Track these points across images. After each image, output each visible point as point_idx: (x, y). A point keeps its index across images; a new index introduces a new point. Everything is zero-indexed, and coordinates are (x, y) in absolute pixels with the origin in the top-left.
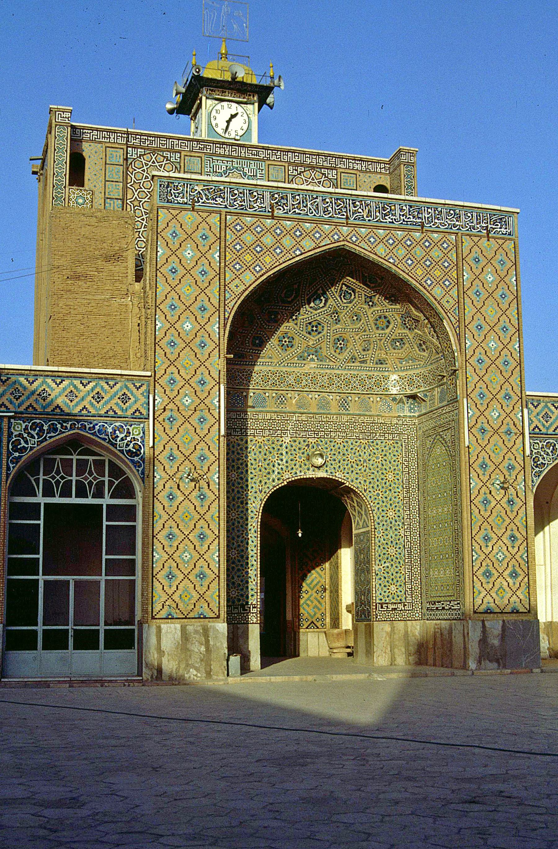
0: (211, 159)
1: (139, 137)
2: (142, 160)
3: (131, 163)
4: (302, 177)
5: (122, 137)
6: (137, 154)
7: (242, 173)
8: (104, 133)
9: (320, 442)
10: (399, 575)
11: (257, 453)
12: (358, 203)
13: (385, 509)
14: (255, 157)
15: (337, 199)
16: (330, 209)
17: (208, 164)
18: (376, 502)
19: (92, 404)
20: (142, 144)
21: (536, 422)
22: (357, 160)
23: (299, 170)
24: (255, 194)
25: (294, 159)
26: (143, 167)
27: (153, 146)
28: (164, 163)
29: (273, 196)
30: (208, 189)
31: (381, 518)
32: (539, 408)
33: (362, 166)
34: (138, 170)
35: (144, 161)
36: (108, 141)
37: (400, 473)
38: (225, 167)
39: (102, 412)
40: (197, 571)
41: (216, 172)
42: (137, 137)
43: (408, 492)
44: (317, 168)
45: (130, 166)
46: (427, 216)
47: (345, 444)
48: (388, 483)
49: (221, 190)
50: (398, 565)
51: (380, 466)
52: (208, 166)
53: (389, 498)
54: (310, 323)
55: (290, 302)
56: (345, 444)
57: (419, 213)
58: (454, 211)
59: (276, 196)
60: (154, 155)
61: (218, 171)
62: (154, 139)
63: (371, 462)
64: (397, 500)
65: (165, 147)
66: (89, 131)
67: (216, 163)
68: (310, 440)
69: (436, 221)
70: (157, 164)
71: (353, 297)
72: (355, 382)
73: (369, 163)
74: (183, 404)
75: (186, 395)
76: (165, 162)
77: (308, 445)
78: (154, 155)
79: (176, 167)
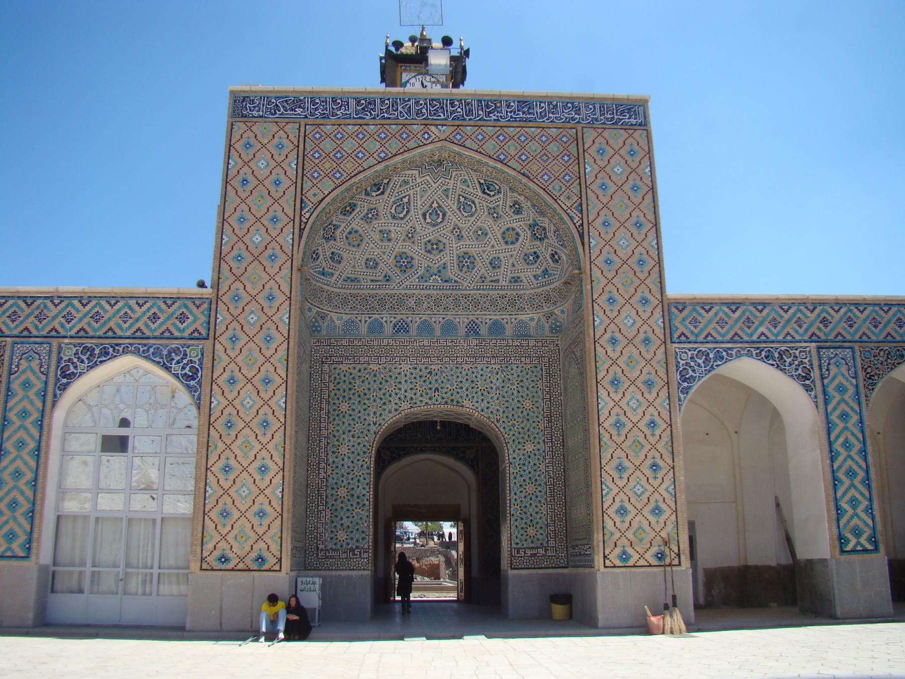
9: (444, 369)
10: (539, 516)
11: (372, 382)
12: (456, 103)
13: (522, 441)
15: (433, 100)
16: (424, 111)
18: (511, 433)
19: (147, 326)
21: (682, 329)
24: (339, 101)
29: (359, 102)
30: (286, 101)
31: (517, 451)
32: (686, 312)
37: (540, 401)
39: (157, 334)
40: (255, 508)
43: (550, 421)
46: (539, 111)
47: (474, 370)
48: (525, 413)
49: (300, 100)
50: (539, 505)
51: (515, 392)
53: (526, 429)
54: (429, 241)
55: (402, 219)
56: (474, 370)
57: (529, 108)
58: (572, 103)
59: (363, 102)
63: (505, 389)
64: (536, 431)
68: (432, 367)
69: (551, 115)
71: (474, 209)
72: (485, 303)
74: (248, 322)
75: (252, 312)
77: (430, 373)
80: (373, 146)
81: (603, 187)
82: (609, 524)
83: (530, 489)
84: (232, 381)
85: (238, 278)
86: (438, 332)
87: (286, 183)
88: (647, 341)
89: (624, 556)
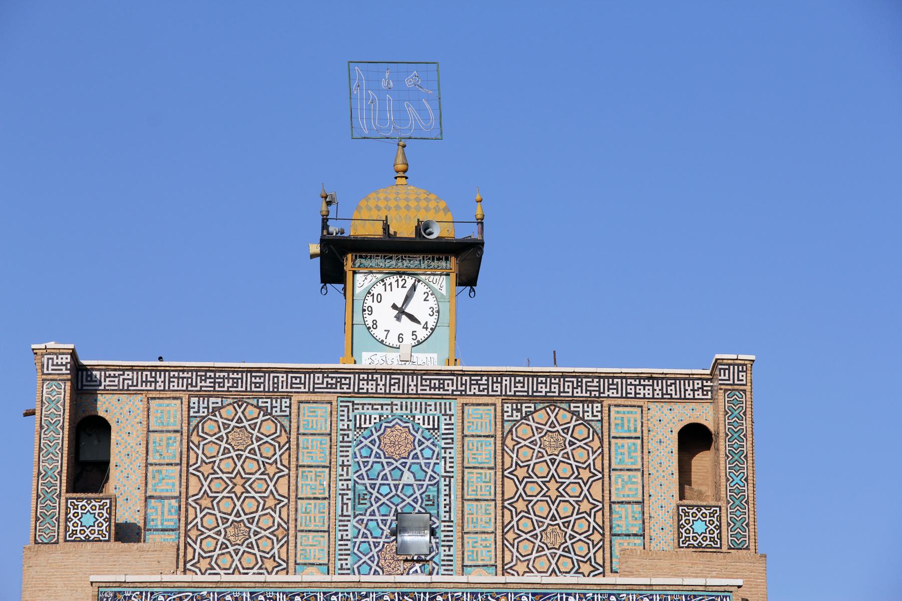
0: (350, 404)
1: (212, 374)
2: (218, 418)
3: (197, 425)
4: (531, 423)
5: (178, 378)
6: (208, 408)
7: (410, 425)
8: (145, 373)
14: (437, 392)
17: (345, 413)
20: (217, 388)
22: (644, 379)
23: (524, 410)
25: (513, 389)
26: (220, 431)
27: (239, 389)
28: (259, 421)
33: (654, 390)
34: (210, 439)
35: (220, 421)
36: (153, 388)
38: (378, 417)
41: (360, 428)
42: (208, 374)
44: (562, 402)
45: (195, 432)
52: (345, 418)
60: (240, 407)
61: (363, 426)
62: (240, 376)
65: (262, 389)
66: (117, 373)
67: (361, 411)
70: (246, 424)
73: (669, 382)
76: (261, 418)
78: (240, 407)
79: (282, 426)
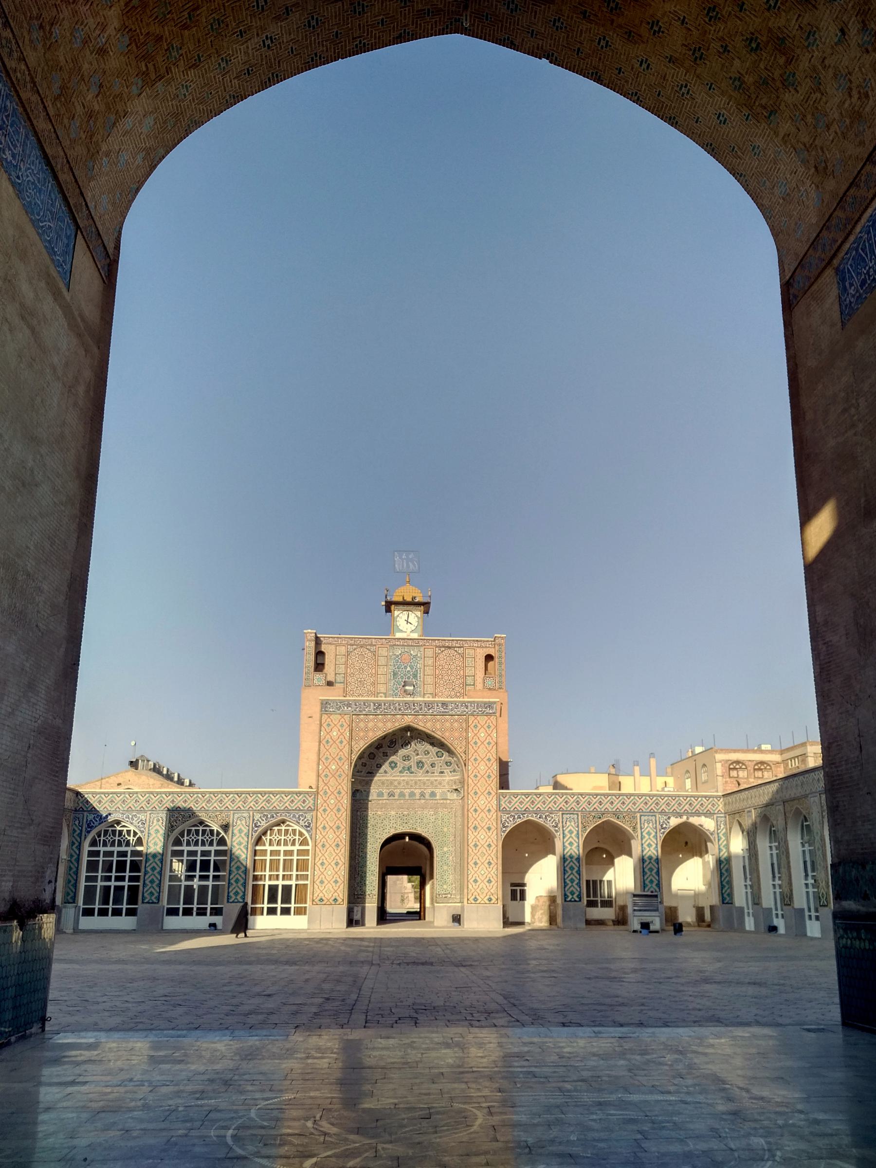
21: (504, 805)
80: (380, 725)
81: (476, 743)
82: (470, 886)
83: (445, 868)
84: (324, 828)
85: (326, 784)
86: (407, 797)
87: (345, 742)
88: (489, 811)
89: (476, 899)
